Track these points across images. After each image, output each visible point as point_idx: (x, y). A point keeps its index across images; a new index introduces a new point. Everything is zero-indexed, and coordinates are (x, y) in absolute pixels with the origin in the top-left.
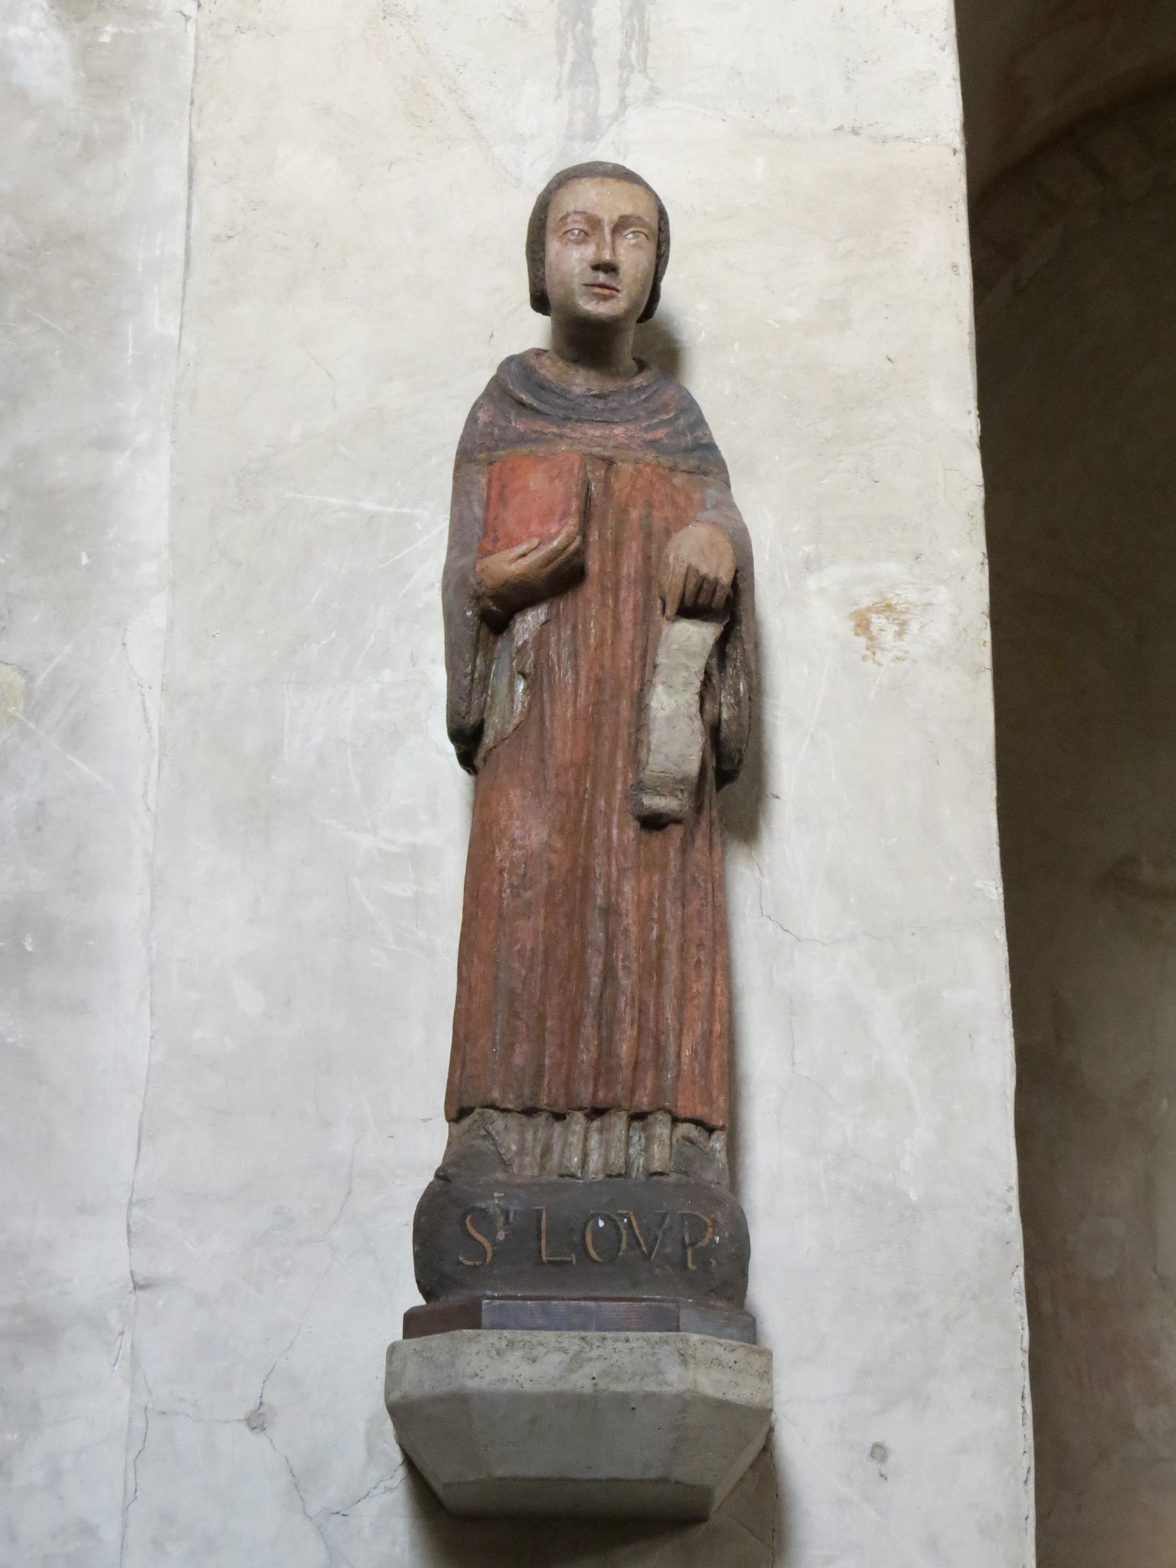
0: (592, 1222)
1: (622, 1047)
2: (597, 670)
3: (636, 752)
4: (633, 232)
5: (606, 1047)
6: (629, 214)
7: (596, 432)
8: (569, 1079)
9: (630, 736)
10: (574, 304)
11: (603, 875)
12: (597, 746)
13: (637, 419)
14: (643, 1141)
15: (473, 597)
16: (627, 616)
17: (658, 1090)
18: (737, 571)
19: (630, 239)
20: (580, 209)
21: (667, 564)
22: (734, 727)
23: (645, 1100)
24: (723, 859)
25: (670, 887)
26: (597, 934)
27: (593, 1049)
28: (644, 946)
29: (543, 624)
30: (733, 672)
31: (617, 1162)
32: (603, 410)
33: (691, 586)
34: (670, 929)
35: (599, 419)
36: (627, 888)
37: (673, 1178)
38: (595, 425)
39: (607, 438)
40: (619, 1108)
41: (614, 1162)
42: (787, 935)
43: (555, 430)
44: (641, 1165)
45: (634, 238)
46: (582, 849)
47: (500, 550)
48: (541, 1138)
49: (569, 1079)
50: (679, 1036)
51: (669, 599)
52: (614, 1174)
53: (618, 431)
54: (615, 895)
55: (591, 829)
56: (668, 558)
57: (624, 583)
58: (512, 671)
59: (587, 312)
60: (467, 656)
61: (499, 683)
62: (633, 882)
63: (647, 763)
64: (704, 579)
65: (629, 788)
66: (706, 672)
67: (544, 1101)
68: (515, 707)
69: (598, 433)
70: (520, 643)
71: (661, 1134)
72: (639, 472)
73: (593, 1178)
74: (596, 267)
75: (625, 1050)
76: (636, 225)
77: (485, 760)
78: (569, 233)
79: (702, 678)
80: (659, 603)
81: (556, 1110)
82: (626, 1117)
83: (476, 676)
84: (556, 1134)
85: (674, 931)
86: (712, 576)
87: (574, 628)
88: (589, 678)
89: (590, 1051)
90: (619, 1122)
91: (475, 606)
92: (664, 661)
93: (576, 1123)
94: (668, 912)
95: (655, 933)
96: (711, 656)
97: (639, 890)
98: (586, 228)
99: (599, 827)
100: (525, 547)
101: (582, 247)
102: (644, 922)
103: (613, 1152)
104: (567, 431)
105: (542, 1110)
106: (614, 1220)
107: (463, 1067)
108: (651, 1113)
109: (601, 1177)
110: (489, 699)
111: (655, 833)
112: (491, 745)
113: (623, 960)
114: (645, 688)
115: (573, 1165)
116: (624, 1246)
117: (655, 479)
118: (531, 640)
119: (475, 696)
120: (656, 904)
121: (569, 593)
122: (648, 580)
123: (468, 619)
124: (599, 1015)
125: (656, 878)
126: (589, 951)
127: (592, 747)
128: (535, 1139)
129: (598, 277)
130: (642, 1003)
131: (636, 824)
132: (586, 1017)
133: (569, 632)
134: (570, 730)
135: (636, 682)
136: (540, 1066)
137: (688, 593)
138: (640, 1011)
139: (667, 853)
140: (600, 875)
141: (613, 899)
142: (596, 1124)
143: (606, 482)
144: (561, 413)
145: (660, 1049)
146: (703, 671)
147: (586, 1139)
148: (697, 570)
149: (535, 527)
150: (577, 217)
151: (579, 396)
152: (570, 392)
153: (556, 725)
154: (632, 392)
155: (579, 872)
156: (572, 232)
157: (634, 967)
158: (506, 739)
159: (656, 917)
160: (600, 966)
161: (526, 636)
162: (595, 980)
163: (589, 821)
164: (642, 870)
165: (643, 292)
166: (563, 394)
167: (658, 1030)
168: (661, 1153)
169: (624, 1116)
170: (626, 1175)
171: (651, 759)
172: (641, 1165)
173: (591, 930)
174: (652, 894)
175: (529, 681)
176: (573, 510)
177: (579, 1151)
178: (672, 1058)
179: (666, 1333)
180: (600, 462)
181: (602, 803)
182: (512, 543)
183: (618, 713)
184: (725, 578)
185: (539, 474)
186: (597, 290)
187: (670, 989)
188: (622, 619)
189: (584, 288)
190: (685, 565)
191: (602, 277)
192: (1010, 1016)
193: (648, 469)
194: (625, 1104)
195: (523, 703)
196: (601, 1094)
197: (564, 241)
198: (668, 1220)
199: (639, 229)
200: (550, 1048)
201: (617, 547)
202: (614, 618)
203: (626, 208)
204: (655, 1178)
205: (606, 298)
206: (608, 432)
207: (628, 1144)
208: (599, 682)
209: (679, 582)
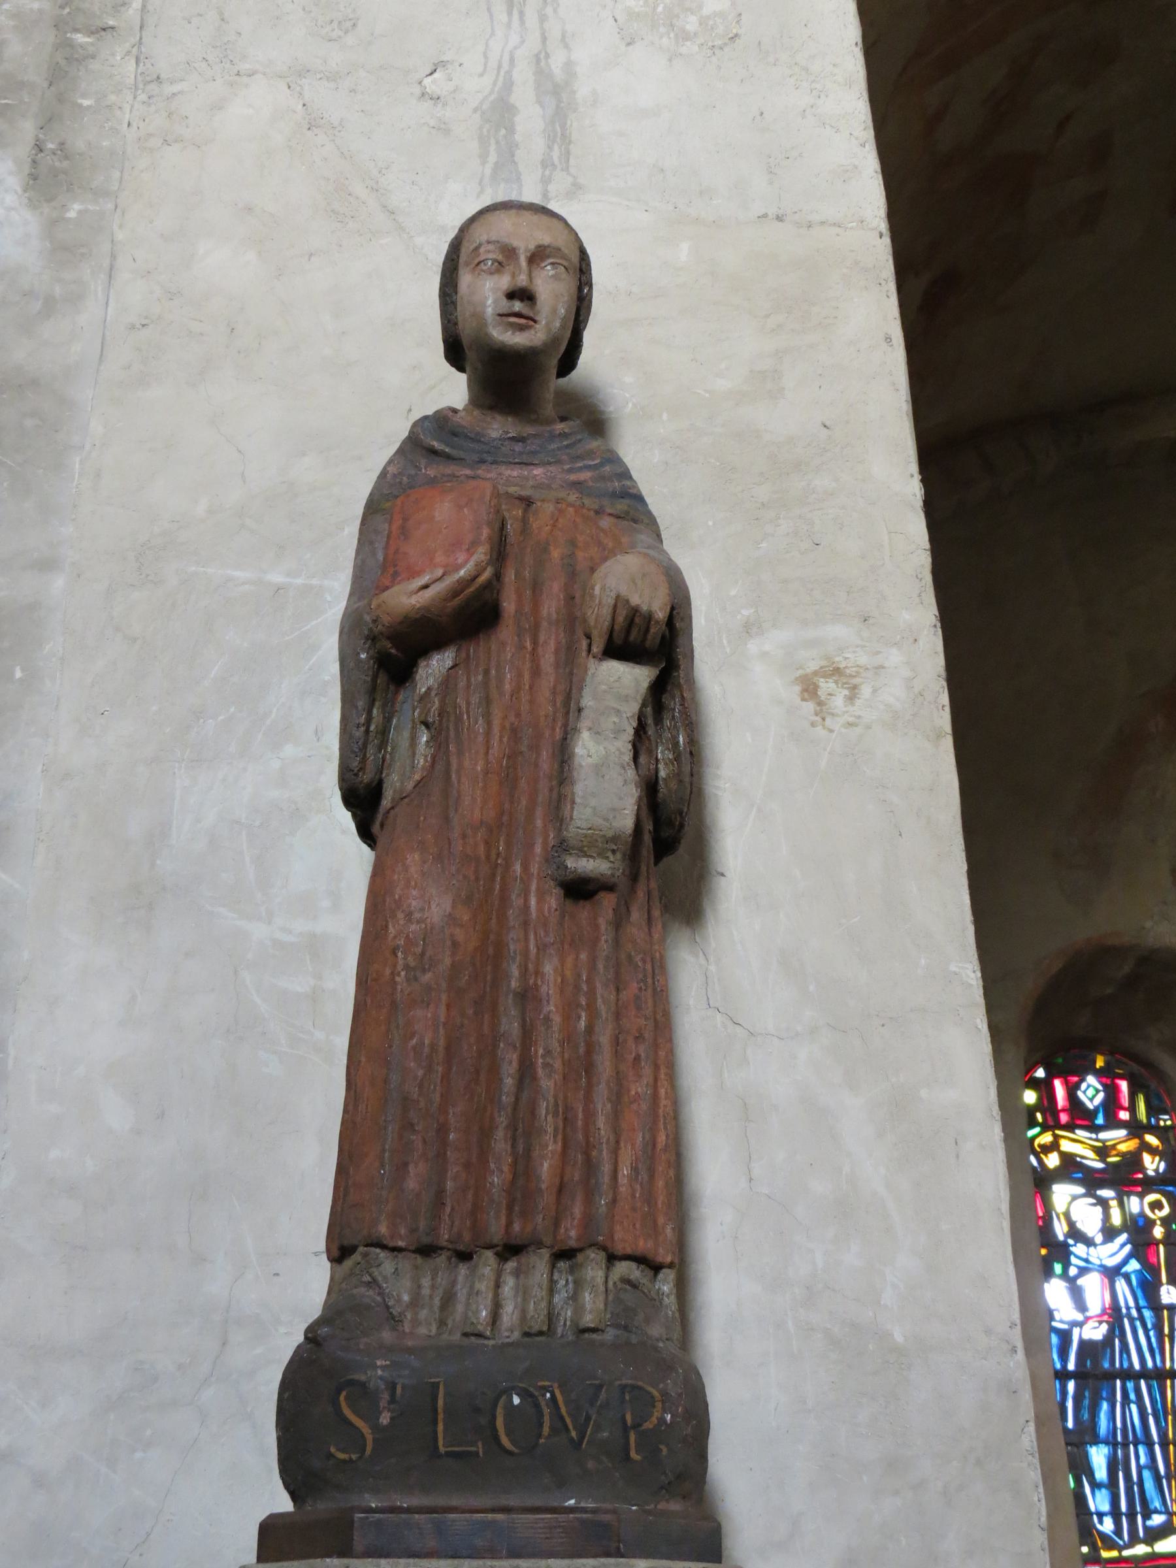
0: (504, 1397)
1: (542, 1165)
2: (512, 718)
3: (558, 808)
4: (552, 264)
5: (523, 1166)
6: (546, 244)
7: (515, 472)
8: (476, 1208)
9: (551, 790)
10: (486, 334)
11: (517, 952)
12: (512, 802)
13: (559, 462)
14: (571, 1286)
15: (367, 638)
16: (548, 660)
17: (588, 1221)
18: (673, 609)
19: (549, 270)
20: (494, 238)
21: (592, 596)
22: (673, 785)
23: (573, 1233)
24: (663, 940)
25: (600, 966)
26: (511, 1026)
27: (506, 1169)
28: (568, 1039)
29: (450, 669)
30: (670, 723)
31: (537, 1316)
32: (521, 453)
33: (620, 619)
34: (601, 1017)
35: (517, 460)
36: (548, 968)
37: (610, 1335)
38: (512, 466)
39: (527, 478)
40: (540, 1244)
41: (533, 1316)
42: (738, 1029)
43: (468, 472)
44: (568, 1319)
45: (553, 269)
46: (494, 921)
47: (399, 583)
48: (440, 1284)
49: (476, 1208)
50: (615, 1152)
51: (595, 634)
52: (533, 1331)
53: (537, 471)
54: (533, 977)
55: (504, 899)
56: (593, 589)
57: (545, 624)
58: (413, 721)
59: (502, 343)
60: (360, 704)
61: (400, 737)
62: (556, 960)
63: (571, 818)
64: (635, 611)
65: (550, 849)
66: (639, 719)
67: (444, 1237)
68: (416, 762)
69: (515, 473)
70: (423, 690)
71: (593, 1278)
72: (561, 511)
73: (508, 1337)
74: (511, 295)
75: (546, 1169)
76: (554, 257)
77: (382, 825)
78: (482, 264)
79: (635, 724)
80: (584, 643)
81: (461, 1247)
82: (548, 1255)
83: (372, 728)
84: (460, 1279)
85: (607, 1019)
86: (645, 608)
87: (487, 672)
88: (503, 728)
89: (502, 1172)
90: (539, 1263)
91: (370, 648)
92: (590, 703)
93: (485, 1265)
94: (599, 996)
95: (582, 1024)
96: (644, 705)
97: (563, 971)
98: (500, 258)
99: (514, 897)
100: (428, 577)
101: (496, 277)
102: (569, 1010)
103: (532, 1303)
104: (479, 472)
105: (442, 1248)
106: (531, 1395)
107: (346, 1194)
108: (581, 1250)
109: (516, 1335)
110: (388, 756)
111: (581, 903)
112: (389, 805)
113: (543, 1056)
114: (569, 736)
115: (481, 1321)
116: (546, 1430)
117: (578, 520)
118: (436, 686)
119: (371, 750)
120: (585, 987)
121: (481, 636)
122: (572, 620)
123: (360, 661)
124: (513, 1127)
125: (583, 956)
126: (502, 1045)
127: (507, 806)
128: (433, 1287)
129: (513, 306)
130: (568, 1109)
131: (558, 891)
132: (497, 1127)
133: (480, 678)
134: (480, 784)
135: (558, 730)
136: (440, 1193)
137: (616, 627)
138: (565, 1119)
139: (596, 927)
140: (515, 952)
141: (531, 982)
142: (511, 1265)
143: (524, 520)
144: (475, 457)
145: (590, 1167)
146: (636, 717)
147: (497, 1285)
148: (627, 601)
149: (440, 558)
150: (491, 247)
151: (494, 439)
152: (484, 436)
153: (463, 779)
154: (552, 437)
155: (491, 951)
156: (486, 262)
157: (558, 1065)
158: (405, 797)
159: (584, 1003)
160: (515, 1064)
161: (431, 682)
162: (509, 1082)
163: (502, 890)
164: (566, 947)
165: (563, 327)
166: (477, 438)
167: (588, 1142)
168: (594, 1302)
169: (546, 1254)
170: (549, 1332)
171: (575, 813)
172: (568, 1319)
173: (504, 1020)
174: (579, 976)
175: (433, 731)
176: (483, 538)
177: (489, 1302)
178: (606, 1179)
179: (603, 1560)
180: (517, 502)
181: (518, 868)
182: (414, 574)
183: (536, 765)
184: (661, 615)
185: (446, 504)
186: (513, 320)
187: (602, 1093)
188: (542, 662)
189: (498, 318)
190: (613, 595)
191: (518, 306)
192: (998, 1118)
193: (571, 509)
194: (547, 1240)
195: (426, 756)
196: (517, 1227)
197: (477, 272)
198: (603, 1395)
199: (558, 261)
200: (454, 1169)
201: (536, 586)
202: (533, 661)
203: (546, 239)
204: (586, 1335)
205: (522, 328)
206: (526, 473)
207: (551, 1291)
208: (515, 732)
209: (606, 612)
